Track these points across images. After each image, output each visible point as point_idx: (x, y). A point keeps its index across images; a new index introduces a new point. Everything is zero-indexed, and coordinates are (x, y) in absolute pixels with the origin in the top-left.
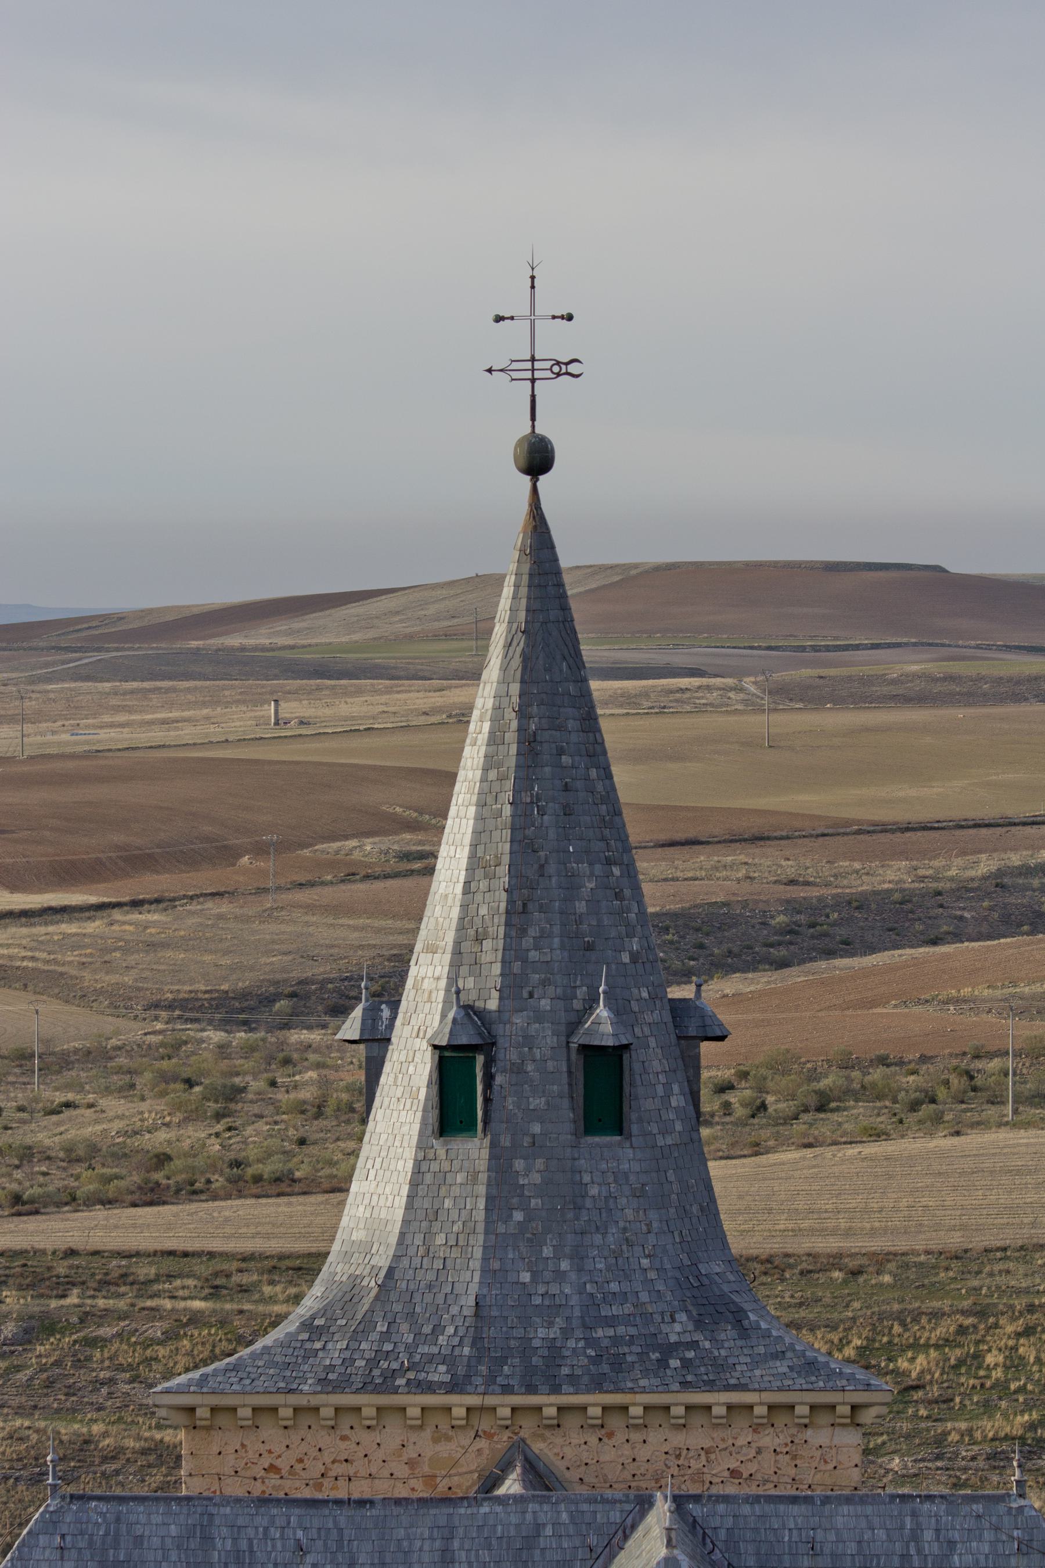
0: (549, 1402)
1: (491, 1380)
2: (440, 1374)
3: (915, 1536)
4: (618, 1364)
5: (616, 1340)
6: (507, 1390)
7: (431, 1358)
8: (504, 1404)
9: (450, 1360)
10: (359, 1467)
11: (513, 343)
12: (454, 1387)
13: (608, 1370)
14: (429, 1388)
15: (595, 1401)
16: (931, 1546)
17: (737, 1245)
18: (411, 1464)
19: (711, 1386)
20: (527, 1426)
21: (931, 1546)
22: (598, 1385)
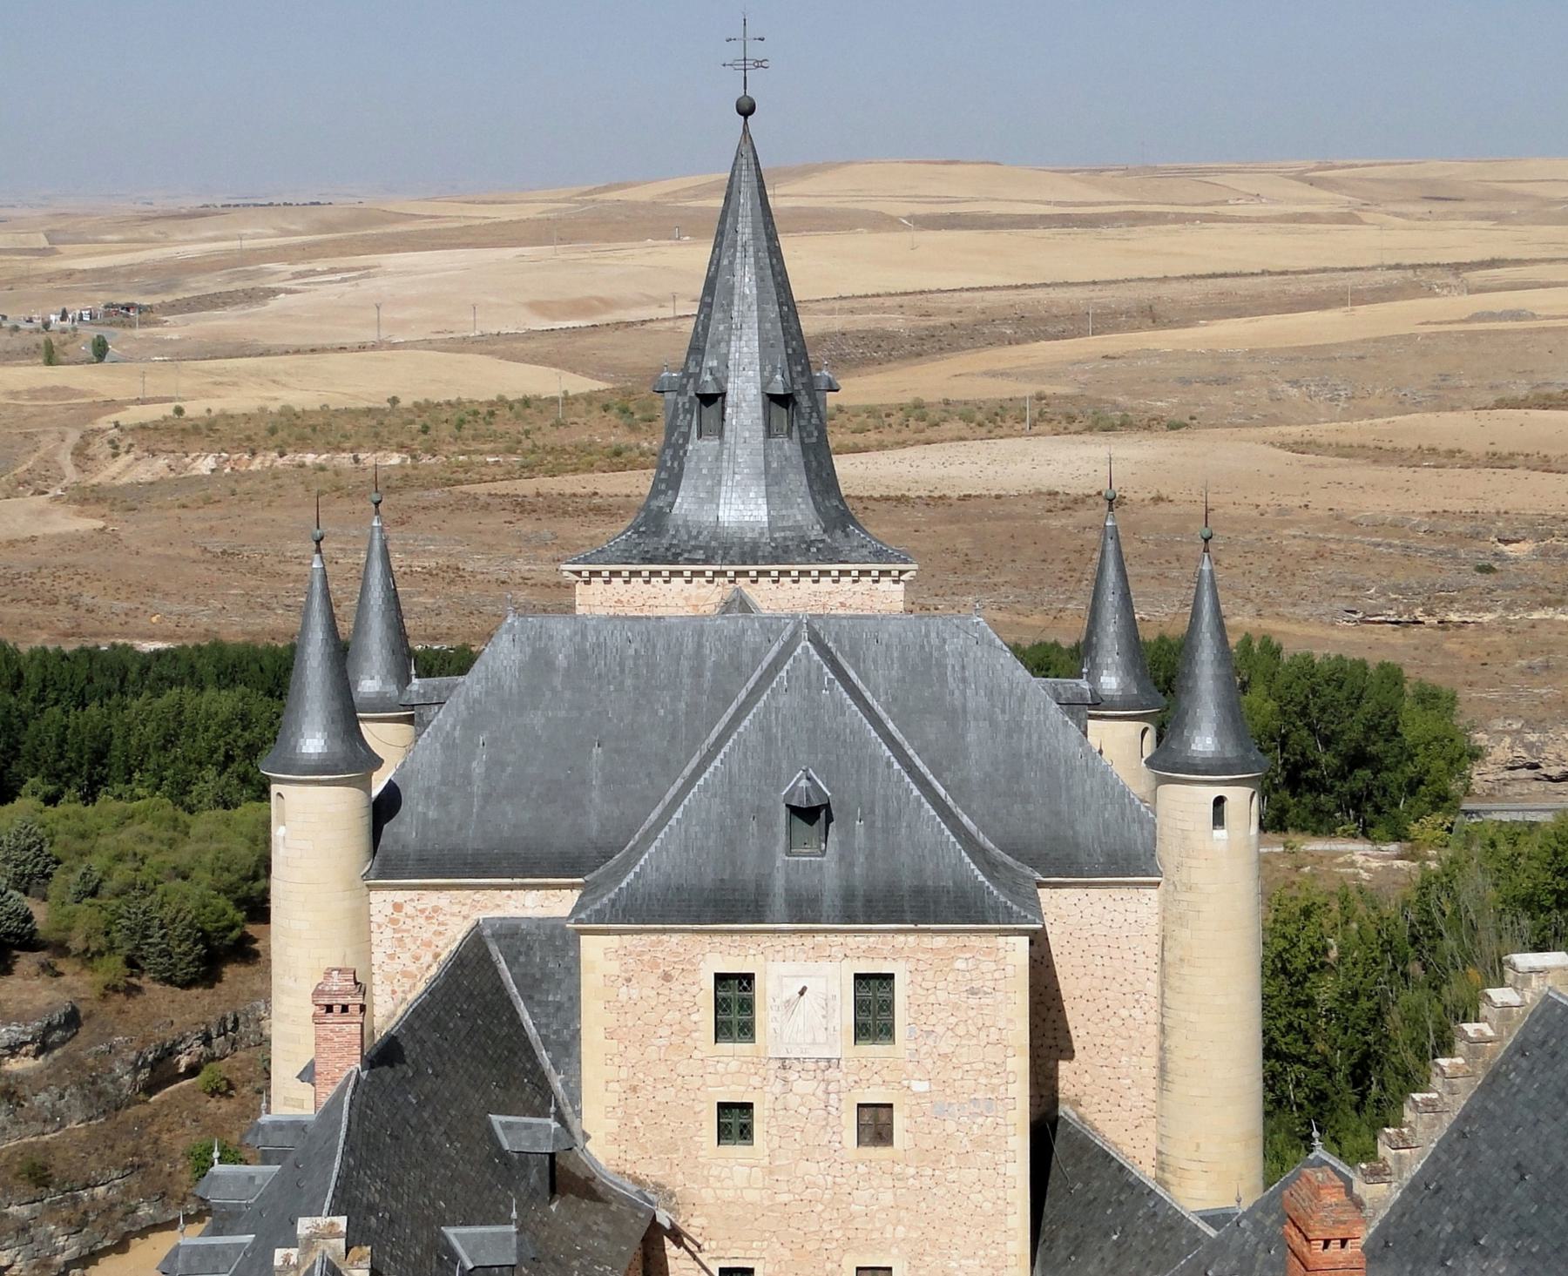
0: (752, 569)
1: (723, 558)
3: (927, 635)
5: (785, 538)
6: (732, 563)
7: (696, 548)
9: (705, 548)
11: (735, 52)
12: (706, 562)
13: (780, 553)
15: (775, 569)
16: (934, 640)
17: (843, 493)
18: (686, 599)
19: (831, 562)
20: (741, 581)
21: (934, 640)
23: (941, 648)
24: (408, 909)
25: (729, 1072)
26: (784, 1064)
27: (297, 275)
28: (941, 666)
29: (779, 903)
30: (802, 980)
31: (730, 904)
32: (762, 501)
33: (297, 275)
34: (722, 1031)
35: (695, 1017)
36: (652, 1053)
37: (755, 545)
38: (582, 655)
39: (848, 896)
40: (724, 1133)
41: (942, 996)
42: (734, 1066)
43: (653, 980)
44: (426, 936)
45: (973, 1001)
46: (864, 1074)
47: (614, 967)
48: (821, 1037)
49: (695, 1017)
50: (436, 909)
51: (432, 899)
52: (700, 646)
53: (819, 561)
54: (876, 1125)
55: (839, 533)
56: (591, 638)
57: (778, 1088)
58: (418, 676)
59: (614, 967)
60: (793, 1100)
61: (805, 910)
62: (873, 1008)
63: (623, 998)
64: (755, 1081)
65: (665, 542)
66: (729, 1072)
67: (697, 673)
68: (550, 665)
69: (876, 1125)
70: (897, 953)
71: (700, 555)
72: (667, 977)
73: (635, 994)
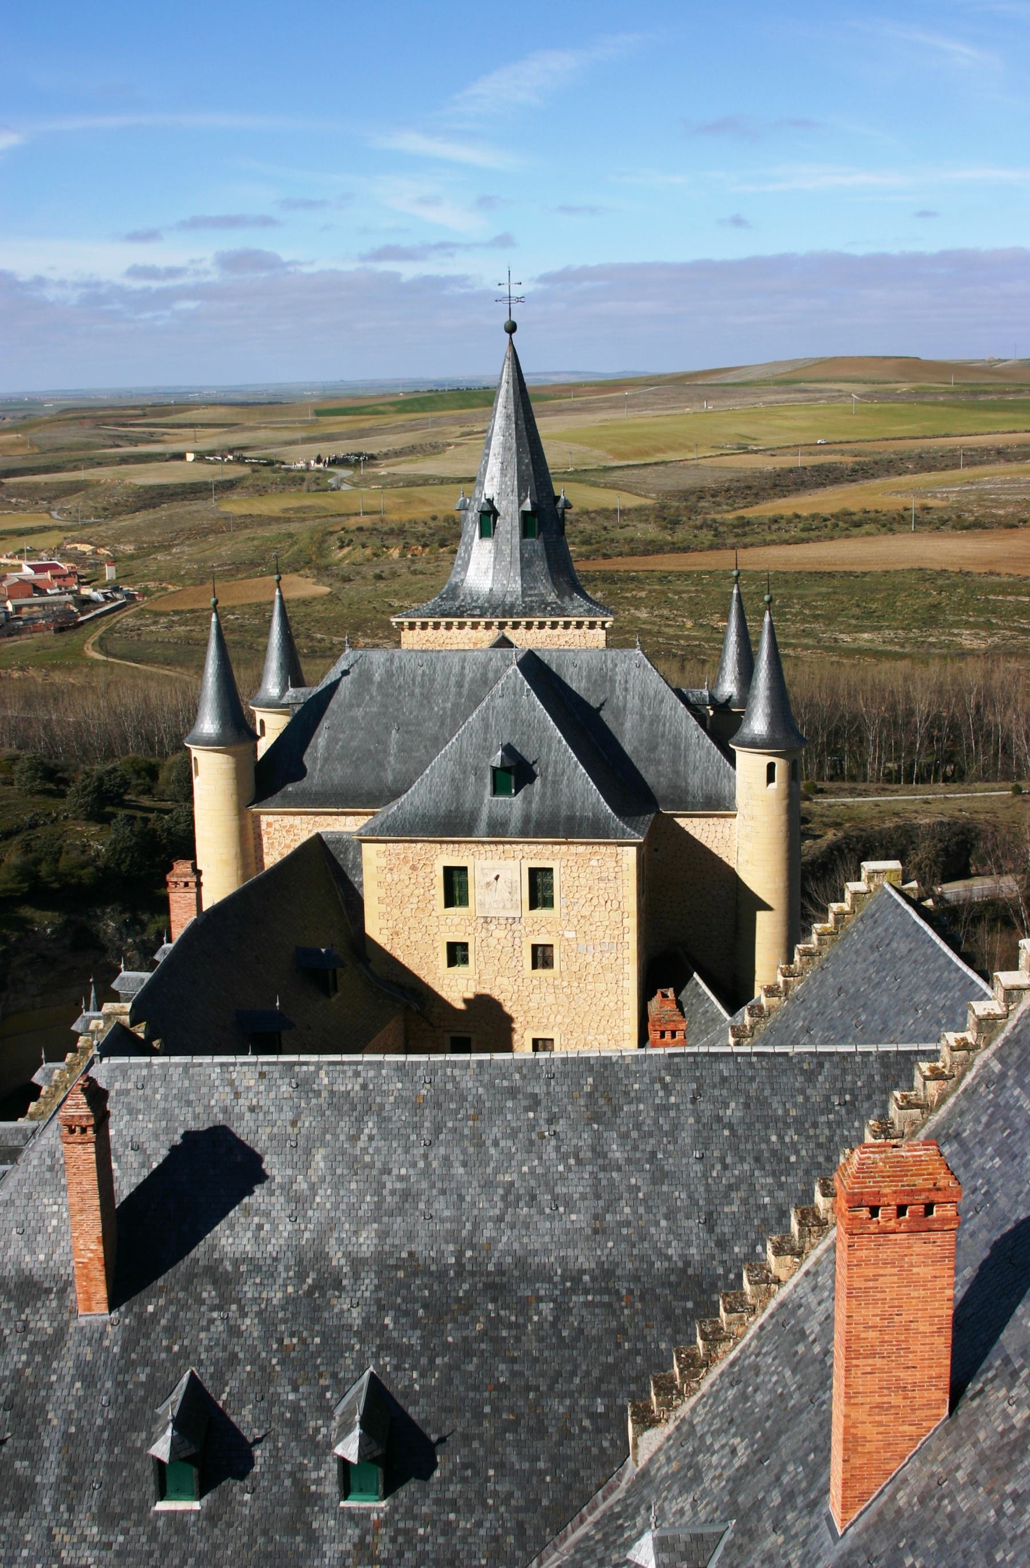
2: (477, 612)
3: (605, 662)
4: (532, 609)
7: (475, 607)
8: (496, 621)
9: (481, 608)
10: (454, 640)
12: (481, 616)
14: (473, 616)
16: (610, 665)
19: (559, 616)
21: (610, 665)
22: (524, 615)
23: (613, 670)
24: (277, 826)
25: (455, 924)
26: (487, 920)
27: (463, 435)
28: (612, 681)
29: (483, 825)
30: (498, 871)
31: (452, 824)
32: (518, 579)
33: (463, 435)
34: (449, 902)
35: (432, 892)
36: (407, 912)
37: (513, 605)
38: (390, 674)
39: (526, 819)
40: (452, 962)
41: (583, 881)
42: (457, 920)
43: (406, 869)
44: (288, 842)
45: (602, 885)
46: (536, 927)
47: (383, 862)
48: (508, 905)
49: (432, 892)
50: (292, 826)
51: (289, 820)
52: (463, 668)
53: (551, 616)
54: (542, 956)
55: (567, 599)
56: (396, 663)
57: (484, 934)
58: (293, 686)
59: (383, 862)
60: (493, 942)
61: (498, 830)
62: (540, 889)
63: (389, 880)
64: (470, 930)
65: (457, 604)
66: (455, 924)
67: (460, 685)
68: (370, 680)
69: (542, 956)
70: (553, 856)
71: (477, 612)
72: (414, 868)
73: (396, 878)
